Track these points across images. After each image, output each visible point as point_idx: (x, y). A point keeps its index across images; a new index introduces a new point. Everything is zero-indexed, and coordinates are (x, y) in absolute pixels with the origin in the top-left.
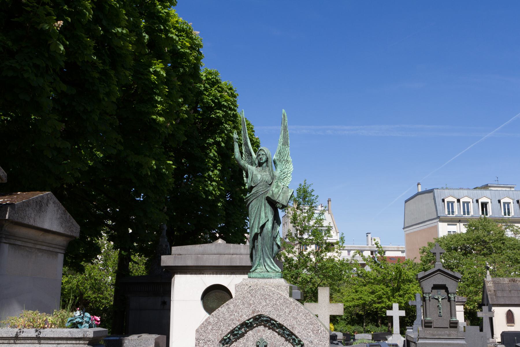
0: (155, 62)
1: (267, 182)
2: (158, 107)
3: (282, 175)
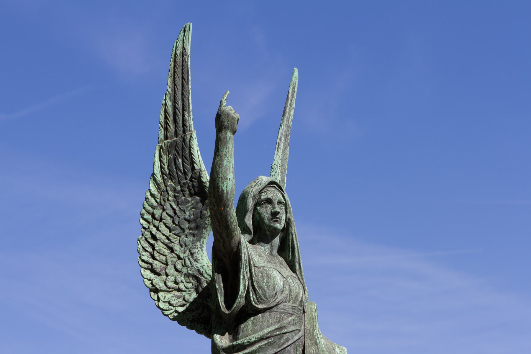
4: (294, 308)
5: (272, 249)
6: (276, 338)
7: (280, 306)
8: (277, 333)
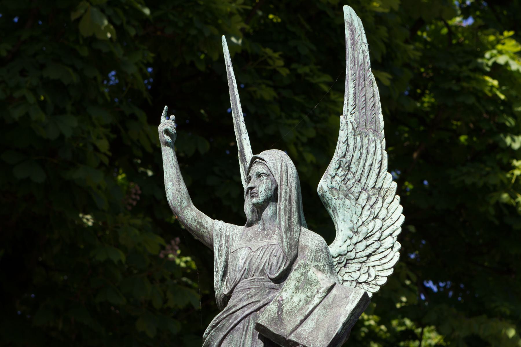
0: (492, 38)
1: (263, 272)
2: (514, 168)
3: (361, 246)
4: (252, 281)
5: (264, 224)
6: (224, 320)
7: (238, 285)
8: (224, 316)
